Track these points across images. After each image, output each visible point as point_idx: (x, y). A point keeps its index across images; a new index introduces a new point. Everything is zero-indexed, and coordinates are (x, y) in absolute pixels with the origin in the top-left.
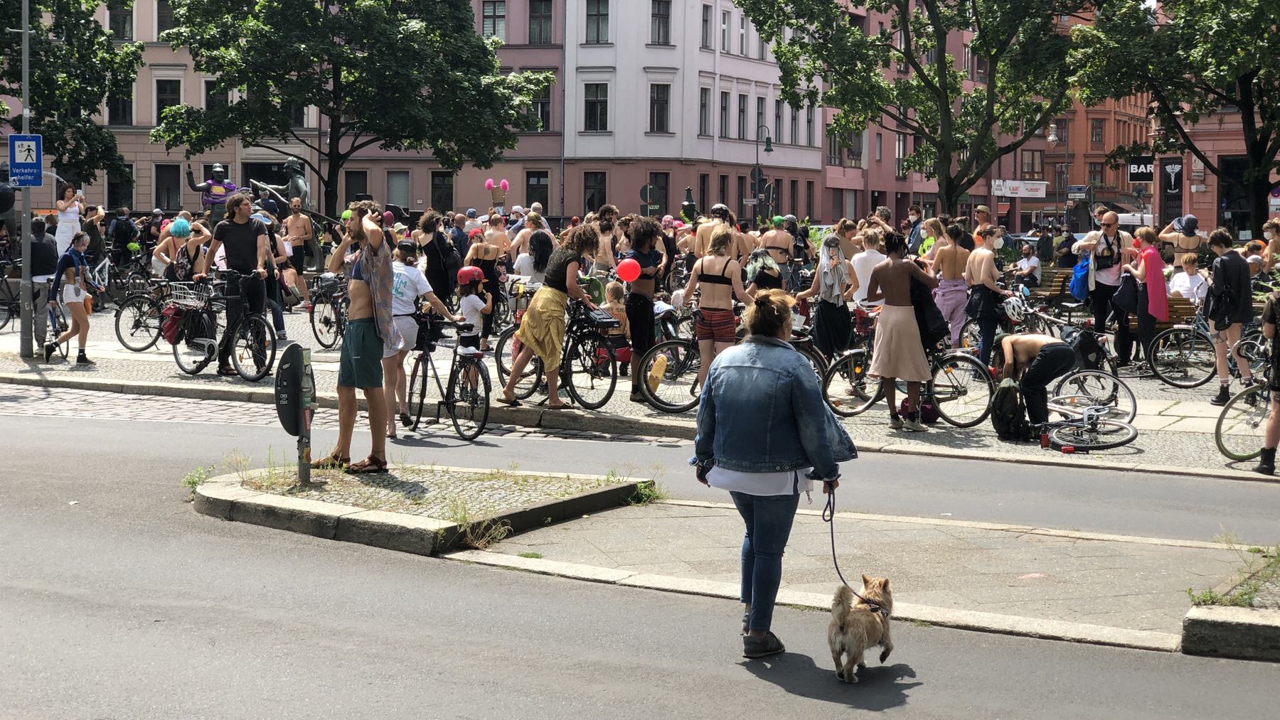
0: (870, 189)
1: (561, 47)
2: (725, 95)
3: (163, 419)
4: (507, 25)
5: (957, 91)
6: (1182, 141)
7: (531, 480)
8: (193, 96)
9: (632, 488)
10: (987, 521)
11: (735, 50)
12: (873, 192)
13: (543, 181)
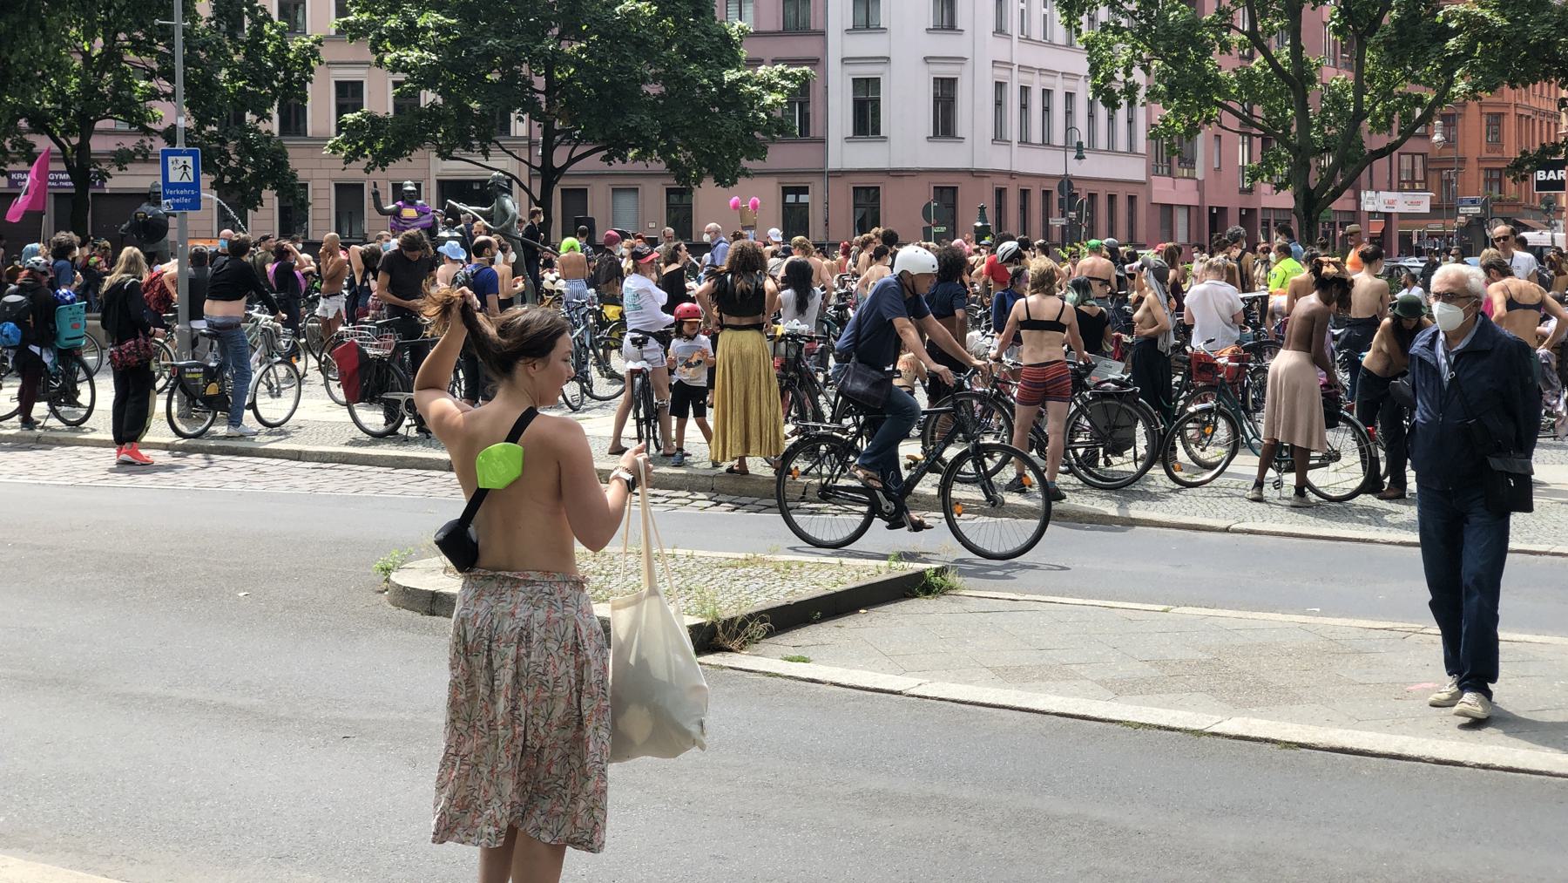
0: (1207, 204)
1: (823, 34)
2: (1025, 90)
3: (349, 492)
4: (756, 7)
5: (1312, 80)
7: (795, 567)
8: (380, 99)
9: (920, 575)
10: (1365, 618)
11: (1037, 34)
12: (1211, 208)
13: (803, 198)
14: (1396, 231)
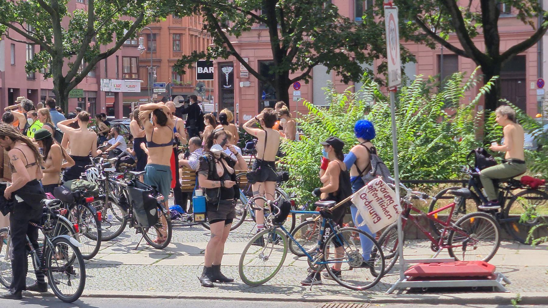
0: (7, 87)
6: (228, 49)
12: (9, 89)
14: (121, 104)
